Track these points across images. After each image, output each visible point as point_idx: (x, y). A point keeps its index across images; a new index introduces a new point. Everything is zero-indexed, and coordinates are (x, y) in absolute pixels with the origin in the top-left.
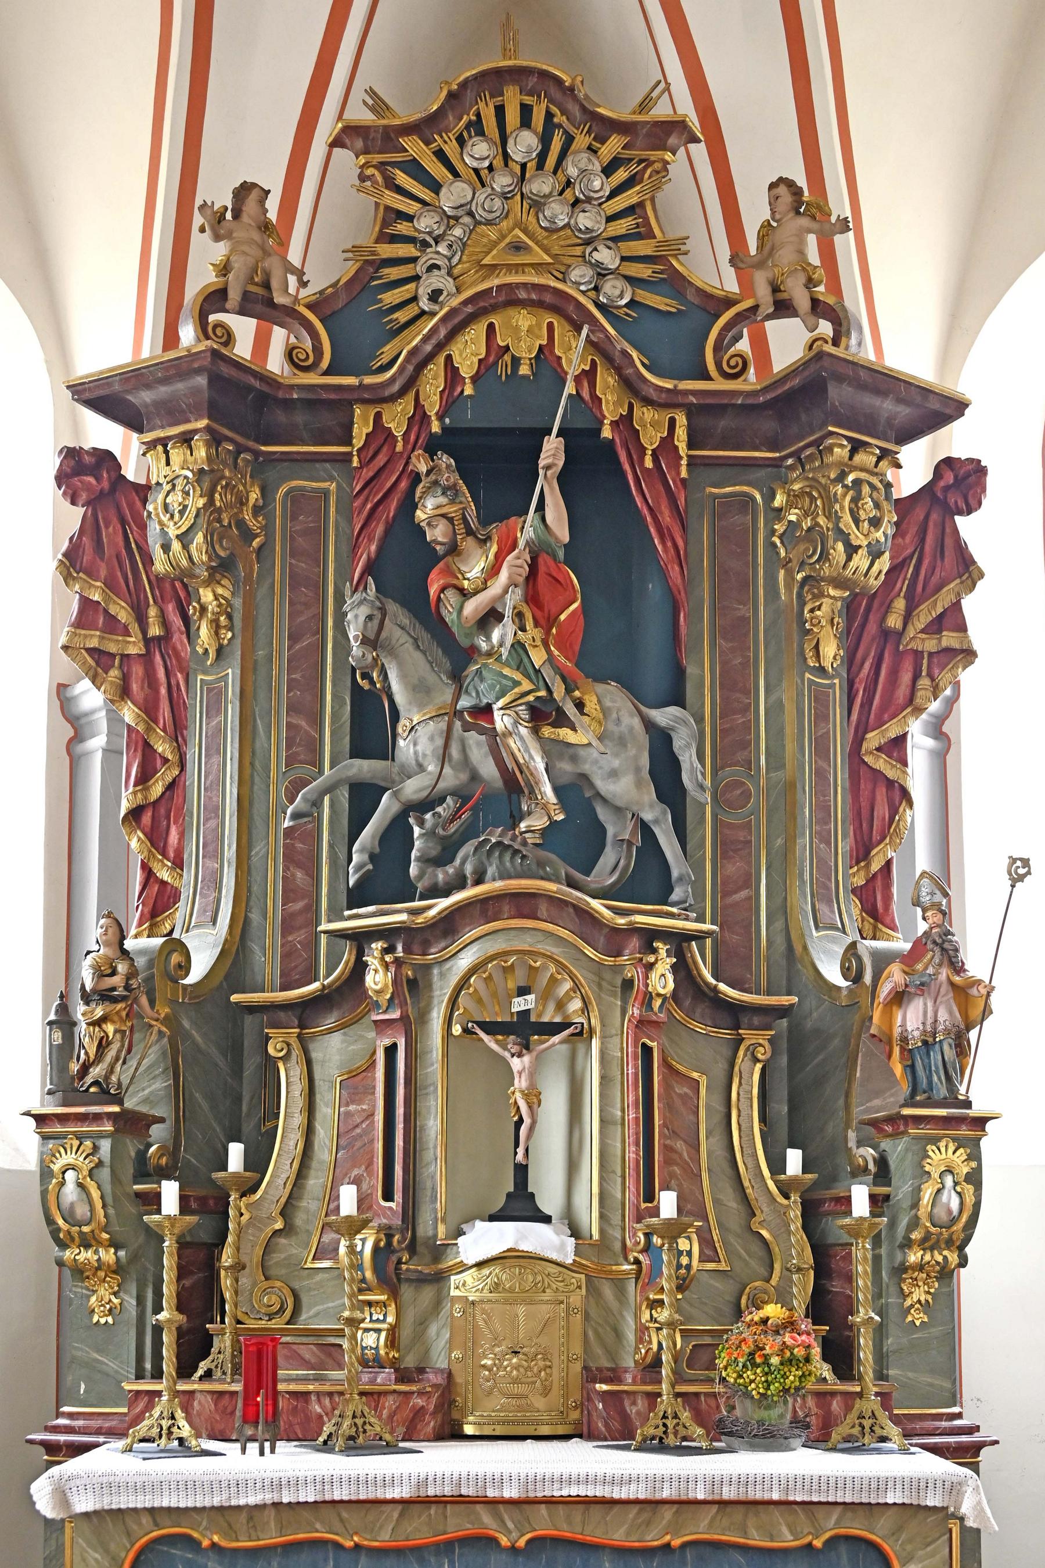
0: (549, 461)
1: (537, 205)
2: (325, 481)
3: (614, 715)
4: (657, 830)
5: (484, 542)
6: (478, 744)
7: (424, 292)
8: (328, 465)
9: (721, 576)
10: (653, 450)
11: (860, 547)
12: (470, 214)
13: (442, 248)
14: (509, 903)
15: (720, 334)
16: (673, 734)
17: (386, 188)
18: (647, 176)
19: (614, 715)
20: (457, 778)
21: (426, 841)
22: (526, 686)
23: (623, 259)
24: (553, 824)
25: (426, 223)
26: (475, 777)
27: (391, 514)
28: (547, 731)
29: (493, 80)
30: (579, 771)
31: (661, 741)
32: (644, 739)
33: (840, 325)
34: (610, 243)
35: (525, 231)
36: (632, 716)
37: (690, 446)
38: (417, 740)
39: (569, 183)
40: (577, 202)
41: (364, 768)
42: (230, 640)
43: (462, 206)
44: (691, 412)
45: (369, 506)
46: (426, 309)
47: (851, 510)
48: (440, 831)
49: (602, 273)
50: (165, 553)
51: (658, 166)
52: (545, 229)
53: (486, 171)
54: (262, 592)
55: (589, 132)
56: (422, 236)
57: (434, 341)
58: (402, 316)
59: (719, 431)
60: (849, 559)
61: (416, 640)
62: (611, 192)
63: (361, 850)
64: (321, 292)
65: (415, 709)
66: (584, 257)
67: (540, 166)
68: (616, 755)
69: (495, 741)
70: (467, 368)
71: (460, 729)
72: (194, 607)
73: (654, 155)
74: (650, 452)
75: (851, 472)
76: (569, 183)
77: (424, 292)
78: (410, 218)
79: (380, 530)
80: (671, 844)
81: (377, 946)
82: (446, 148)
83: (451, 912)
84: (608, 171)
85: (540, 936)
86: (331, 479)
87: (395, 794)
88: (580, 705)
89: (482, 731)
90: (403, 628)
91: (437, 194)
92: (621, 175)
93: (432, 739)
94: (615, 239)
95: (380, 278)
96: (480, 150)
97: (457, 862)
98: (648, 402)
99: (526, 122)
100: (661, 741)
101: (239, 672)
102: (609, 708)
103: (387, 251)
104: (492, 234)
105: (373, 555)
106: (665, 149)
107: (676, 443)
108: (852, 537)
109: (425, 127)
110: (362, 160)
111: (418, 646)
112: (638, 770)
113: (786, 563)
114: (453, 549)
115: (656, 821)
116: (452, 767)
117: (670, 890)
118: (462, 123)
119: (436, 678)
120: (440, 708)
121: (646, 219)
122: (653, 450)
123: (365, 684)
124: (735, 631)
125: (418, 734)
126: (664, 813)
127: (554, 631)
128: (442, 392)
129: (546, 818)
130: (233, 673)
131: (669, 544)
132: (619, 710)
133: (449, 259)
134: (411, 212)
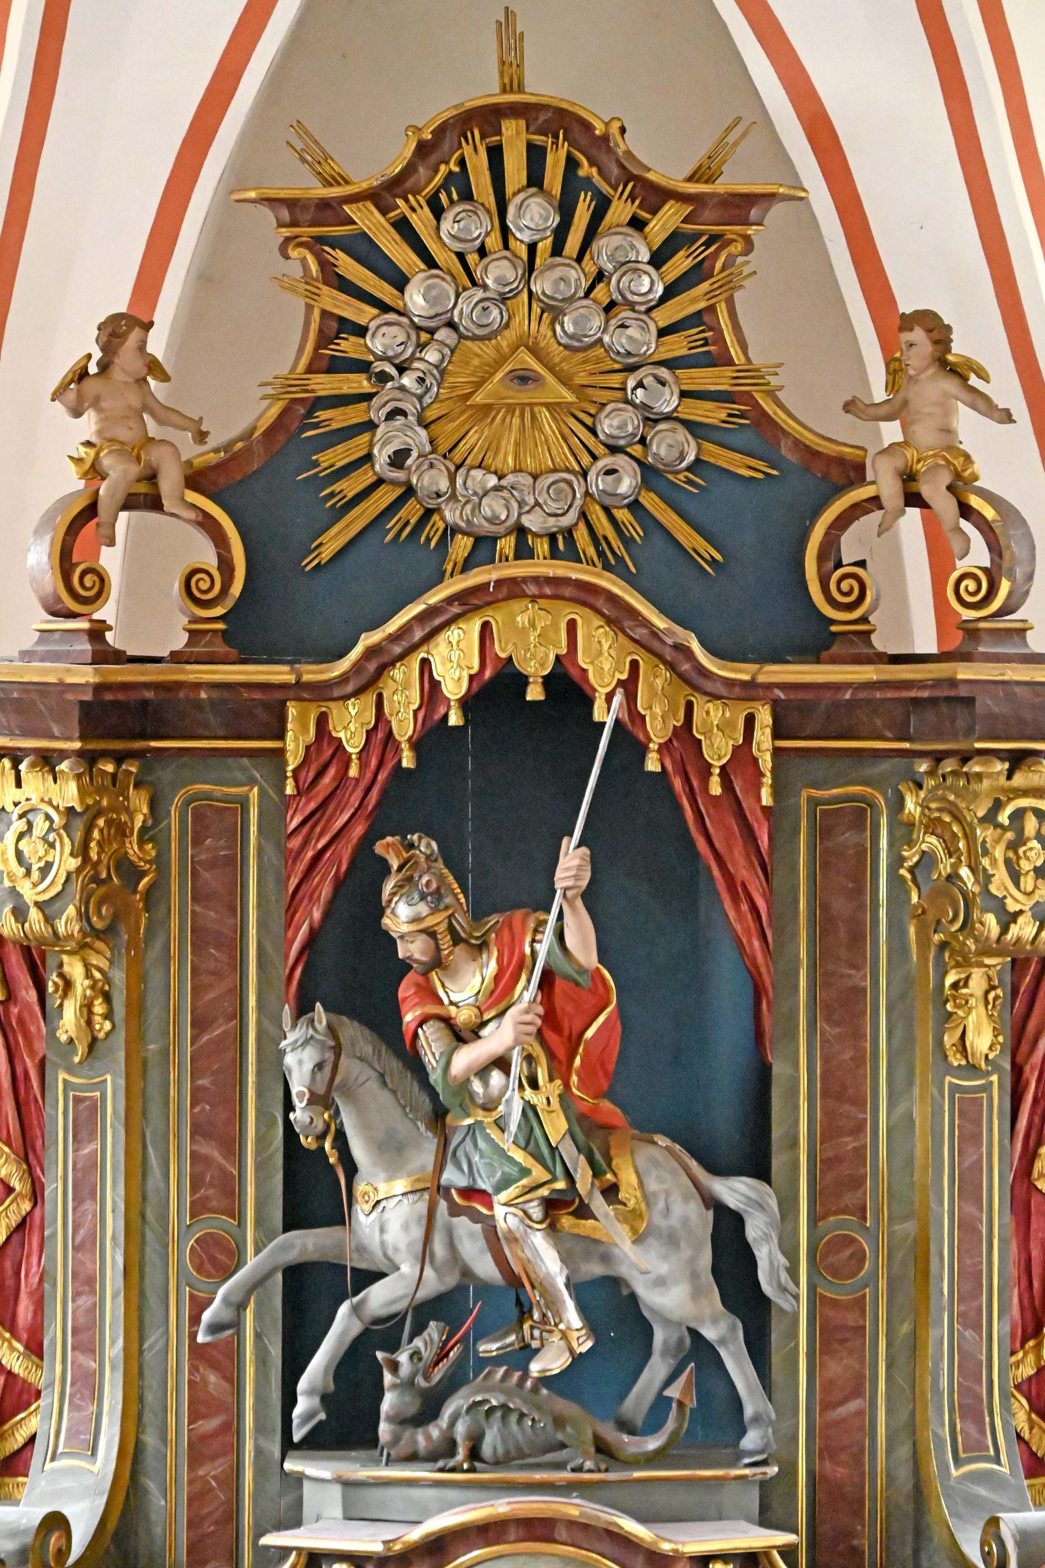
0: (570, 883)
3: (661, 1205)
4: (723, 1353)
5: (482, 947)
6: (472, 1235)
7: (382, 457)
8: (245, 761)
9: (824, 922)
10: (723, 768)
11: (1021, 912)
12: (451, 325)
13: (407, 380)
15: (827, 534)
16: (745, 1216)
17: (324, 283)
18: (719, 265)
19: (661, 1205)
21: (402, 1394)
22: (539, 1173)
23: (683, 394)
24: (578, 1360)
25: (384, 340)
26: (467, 1273)
27: (344, 868)
28: (566, 1222)
31: (728, 1227)
32: (703, 1221)
33: (1000, 556)
34: (664, 373)
35: (535, 351)
36: (686, 1198)
37: (776, 735)
38: (386, 1214)
39: (601, 276)
40: (610, 307)
41: (307, 1243)
42: (108, 1034)
43: (437, 315)
45: (310, 854)
47: (1008, 862)
49: (652, 420)
50: (17, 920)
51: (737, 247)
52: (566, 347)
53: (476, 257)
54: (154, 952)
55: (632, 197)
56: (379, 366)
57: (405, 644)
58: (350, 486)
60: (1005, 930)
61: (382, 1076)
62: (666, 289)
63: (310, 1392)
64: (227, 447)
65: (382, 1175)
66: (624, 389)
67: (557, 250)
68: (665, 1258)
69: (493, 1238)
70: (454, 684)
71: (446, 1212)
72: (55, 983)
73: (730, 230)
74: (717, 771)
75: (1010, 800)
76: (601, 276)
77: (382, 457)
78: (361, 331)
79: (326, 892)
80: (743, 1372)
82: (414, 219)
84: (658, 260)
86: (252, 782)
87: (356, 1309)
88: (611, 1192)
89: (476, 1217)
90: (361, 1059)
91: (402, 291)
92: (680, 263)
94: (670, 364)
95: (316, 426)
96: (460, 227)
97: (444, 1421)
98: (715, 697)
99: (535, 179)
100: (728, 1227)
101: (122, 1082)
102: (654, 1194)
103: (325, 385)
104: (487, 350)
105: (316, 924)
106: (747, 223)
108: (1009, 901)
109: (380, 197)
110: (286, 232)
111: (385, 1083)
112: (694, 1276)
113: (920, 915)
114: (437, 963)
115: (722, 1341)
116: (436, 1270)
117: (742, 1432)
118: (438, 179)
119: (411, 1124)
121: (717, 330)
123: (308, 1142)
124: (843, 1008)
125: (387, 1215)
126: (733, 1328)
127: (578, 1061)
128: (416, 712)
129: (568, 1354)
130: (113, 1082)
131: (745, 907)
132: (668, 1194)
133: (420, 398)
134: (363, 322)
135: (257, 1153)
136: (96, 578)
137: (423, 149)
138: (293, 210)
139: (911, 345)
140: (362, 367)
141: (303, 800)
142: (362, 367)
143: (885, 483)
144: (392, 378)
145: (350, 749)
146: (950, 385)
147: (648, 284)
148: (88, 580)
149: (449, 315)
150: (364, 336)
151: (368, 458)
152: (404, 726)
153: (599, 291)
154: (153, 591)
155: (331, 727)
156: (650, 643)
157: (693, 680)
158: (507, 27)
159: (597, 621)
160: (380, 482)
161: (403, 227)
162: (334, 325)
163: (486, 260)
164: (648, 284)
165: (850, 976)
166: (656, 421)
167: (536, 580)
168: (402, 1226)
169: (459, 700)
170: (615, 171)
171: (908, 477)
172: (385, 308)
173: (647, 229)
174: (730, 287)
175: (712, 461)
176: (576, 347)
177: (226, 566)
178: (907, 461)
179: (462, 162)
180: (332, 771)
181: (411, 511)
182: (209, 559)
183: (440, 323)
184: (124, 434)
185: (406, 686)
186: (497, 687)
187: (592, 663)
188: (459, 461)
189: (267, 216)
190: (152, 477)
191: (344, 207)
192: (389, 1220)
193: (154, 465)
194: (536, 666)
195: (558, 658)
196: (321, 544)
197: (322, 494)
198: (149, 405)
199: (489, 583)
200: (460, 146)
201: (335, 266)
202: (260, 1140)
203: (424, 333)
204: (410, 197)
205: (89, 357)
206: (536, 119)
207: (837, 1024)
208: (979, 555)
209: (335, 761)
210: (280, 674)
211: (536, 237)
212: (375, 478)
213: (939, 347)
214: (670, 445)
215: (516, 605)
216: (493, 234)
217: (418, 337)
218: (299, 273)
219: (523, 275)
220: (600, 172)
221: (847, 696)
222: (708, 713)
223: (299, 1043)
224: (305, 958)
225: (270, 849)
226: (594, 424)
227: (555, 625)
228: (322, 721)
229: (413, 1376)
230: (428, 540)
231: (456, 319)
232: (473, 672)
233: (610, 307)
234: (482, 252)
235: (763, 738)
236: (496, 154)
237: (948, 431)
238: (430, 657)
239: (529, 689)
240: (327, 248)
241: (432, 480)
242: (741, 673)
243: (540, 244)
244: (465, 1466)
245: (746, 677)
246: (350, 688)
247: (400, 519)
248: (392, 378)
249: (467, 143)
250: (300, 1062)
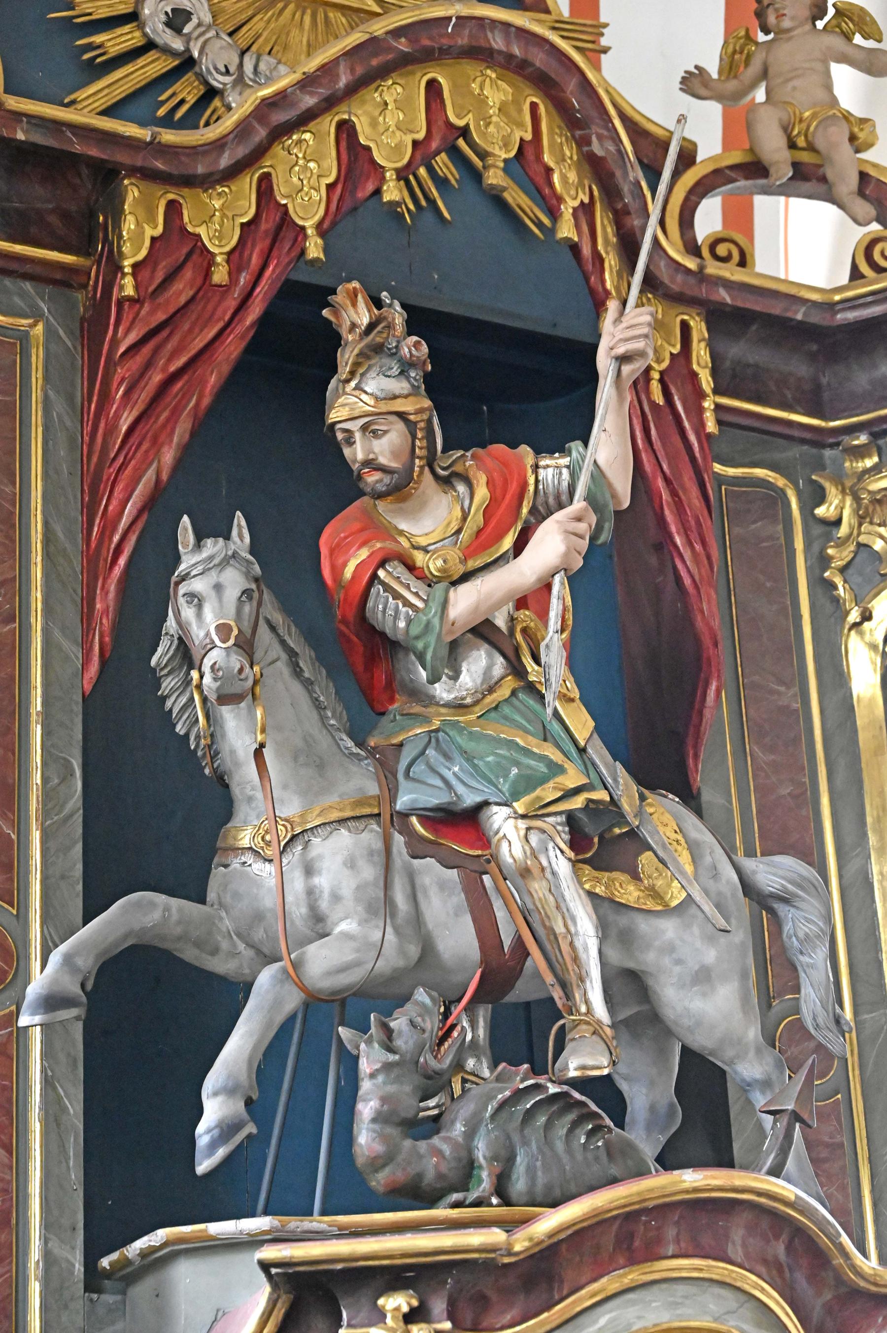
2: (26, 317)
6: (442, 886)
8: (28, 286)
10: (662, 373)
14: (677, 1223)
15: (687, 199)
20: (402, 951)
27: (206, 401)
30: (631, 965)
45: (157, 378)
46: (159, 41)
48: (427, 1058)
63: (229, 1090)
79: (182, 430)
81: (397, 1302)
83: (577, 1233)
85: (730, 1299)
86: (37, 316)
93: (351, 864)
105: (165, 477)
107: (695, 367)
120: (359, 803)
122: (662, 373)
135: (46, 812)
141: (146, 307)
145: (215, 250)
152: (308, 206)
160: (149, 46)
165: (779, 693)
168: (345, 864)
180: (188, 273)
188: (244, 45)
192: (320, 857)
197: (79, 43)
202: (48, 794)
207: (772, 749)
209: (190, 265)
215: (470, 68)
221: (799, 317)
223: (216, 561)
224: (145, 517)
225: (59, 406)
227: (517, 103)
228: (173, 208)
229: (420, 1049)
235: (701, 354)
238: (354, 119)
241: (216, 56)
244: (494, 1201)
246: (225, 161)
247: (174, 94)
250: (218, 588)
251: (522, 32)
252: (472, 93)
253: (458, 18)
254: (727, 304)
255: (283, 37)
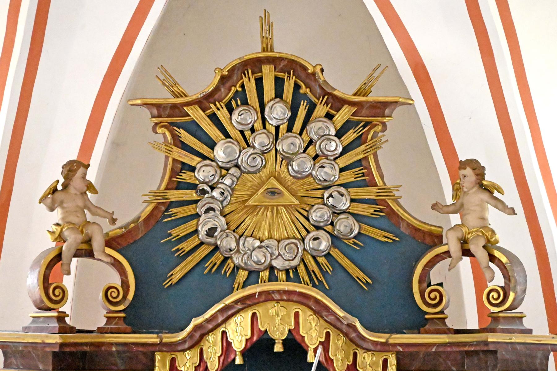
1: (288, 160)
12: (237, 166)
13: (216, 193)
18: (370, 137)
23: (352, 201)
25: (204, 173)
29: (253, 65)
33: (510, 280)
34: (342, 190)
40: (316, 157)
43: (230, 161)
44: (398, 354)
49: (336, 213)
51: (380, 128)
52: (294, 177)
53: (249, 132)
55: (327, 103)
56: (201, 186)
58: (187, 246)
59: (421, 356)
62: (343, 149)
64: (126, 226)
67: (290, 129)
76: (311, 142)
82: (218, 113)
84: (339, 134)
91: (213, 149)
92: (350, 136)
94: (345, 186)
95: (170, 216)
96: (243, 117)
98: (368, 350)
99: (279, 94)
103: (175, 195)
104: (255, 179)
106: (384, 116)
109: (202, 103)
110: (156, 120)
118: (231, 94)
128: (219, 357)
133: (222, 202)
134: (193, 164)
136: (61, 291)
137: (223, 79)
138: (159, 109)
139: (465, 176)
140: (193, 187)
142: (193, 187)
143: (452, 244)
144: (208, 193)
146: (484, 196)
147: (334, 146)
148: (57, 292)
149: (236, 161)
150: (193, 171)
151: (196, 231)
153: (311, 150)
154: (90, 297)
155: (177, 365)
156: (335, 323)
157: (357, 342)
158: (265, 19)
159: (310, 312)
160: (202, 243)
161: (213, 118)
162: (179, 166)
163: (254, 134)
164: (334, 146)
166: (339, 214)
167: (278, 292)
169: (241, 352)
170: (319, 91)
171: (464, 242)
172: (204, 158)
173: (334, 119)
174: (375, 148)
175: (367, 233)
176: (299, 177)
177: (125, 285)
178: (463, 234)
179: (243, 86)
181: (217, 258)
182: (116, 281)
183: (232, 165)
184: (75, 219)
185: (215, 344)
186: (260, 346)
187: (306, 333)
188: (241, 234)
189: (146, 112)
190: (89, 241)
191: (185, 108)
193: (90, 235)
194: (279, 334)
195: (290, 330)
196: (172, 275)
197: (173, 250)
198: (87, 205)
199: (256, 293)
200: (242, 78)
201: (180, 137)
203: (224, 170)
204: (217, 103)
205: (58, 181)
206: (280, 64)
208: (499, 280)
210: (151, 338)
211: (280, 123)
212: (199, 242)
213: (479, 177)
214: (346, 226)
215: (269, 304)
216: (258, 121)
217: (221, 172)
218: (162, 140)
219: (273, 142)
220: (311, 91)
221: (434, 350)
222: (364, 358)
226: (308, 215)
228: (173, 361)
230: (226, 272)
231: (240, 163)
232: (248, 337)
233: (316, 157)
234: (253, 130)
236: (259, 82)
237: (483, 219)
239: (276, 346)
240: (176, 128)
241: (228, 243)
242: (381, 338)
243: (281, 127)
245: (383, 340)
246: (187, 346)
247: (212, 262)
248: (208, 193)
249: (245, 77)
251: (285, 292)
252: (269, 316)
253: (259, 293)
254: (401, 352)
255: (259, 224)
